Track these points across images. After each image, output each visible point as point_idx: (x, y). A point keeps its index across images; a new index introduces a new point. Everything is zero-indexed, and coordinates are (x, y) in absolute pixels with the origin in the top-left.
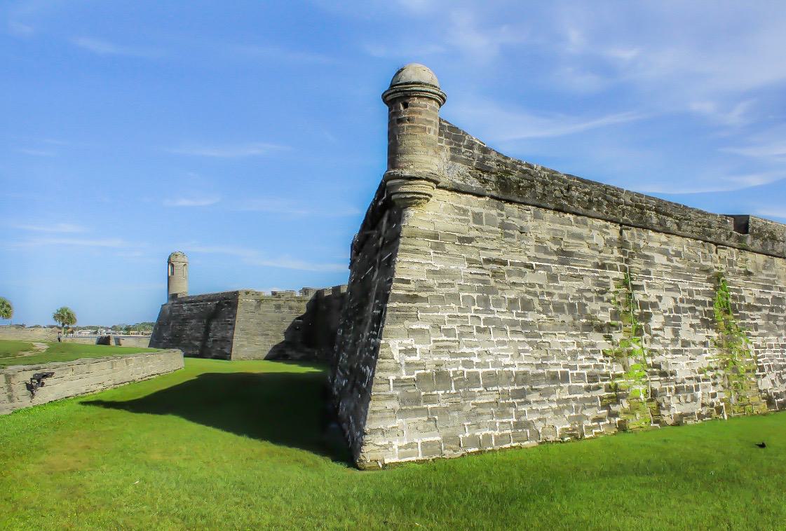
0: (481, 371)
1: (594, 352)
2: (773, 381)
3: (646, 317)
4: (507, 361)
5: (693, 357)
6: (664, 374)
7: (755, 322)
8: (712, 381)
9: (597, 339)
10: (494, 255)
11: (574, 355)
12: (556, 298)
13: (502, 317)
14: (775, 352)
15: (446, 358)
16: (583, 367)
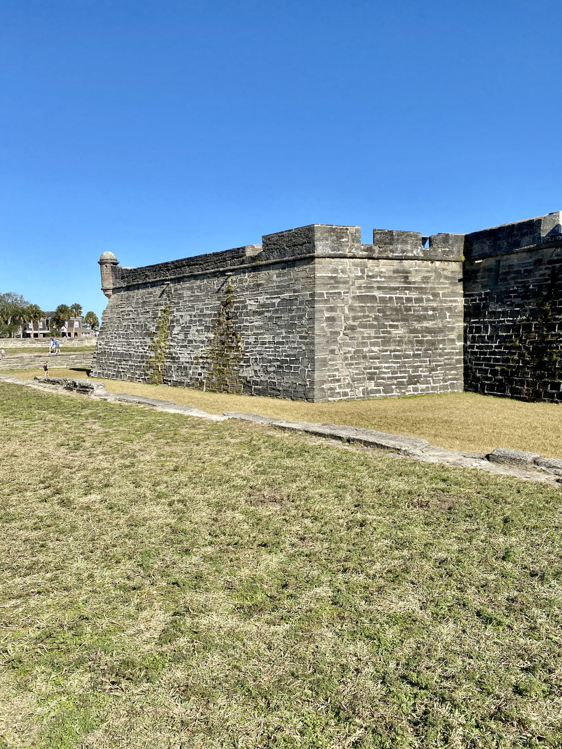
0: (113, 352)
1: (146, 346)
2: (256, 371)
3: (171, 328)
4: (119, 348)
5: (193, 350)
6: (173, 358)
7: (253, 324)
8: (201, 365)
9: (148, 340)
10: (123, 309)
11: (138, 346)
12: (137, 323)
13: (121, 332)
14: (266, 348)
15: (106, 347)
16: (140, 352)
